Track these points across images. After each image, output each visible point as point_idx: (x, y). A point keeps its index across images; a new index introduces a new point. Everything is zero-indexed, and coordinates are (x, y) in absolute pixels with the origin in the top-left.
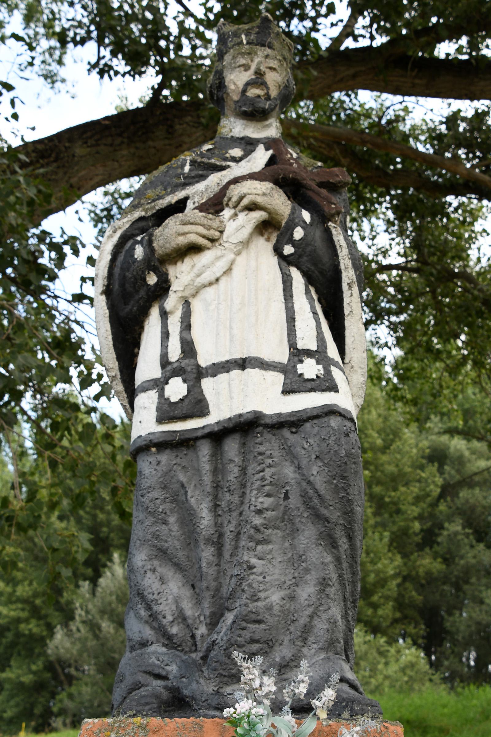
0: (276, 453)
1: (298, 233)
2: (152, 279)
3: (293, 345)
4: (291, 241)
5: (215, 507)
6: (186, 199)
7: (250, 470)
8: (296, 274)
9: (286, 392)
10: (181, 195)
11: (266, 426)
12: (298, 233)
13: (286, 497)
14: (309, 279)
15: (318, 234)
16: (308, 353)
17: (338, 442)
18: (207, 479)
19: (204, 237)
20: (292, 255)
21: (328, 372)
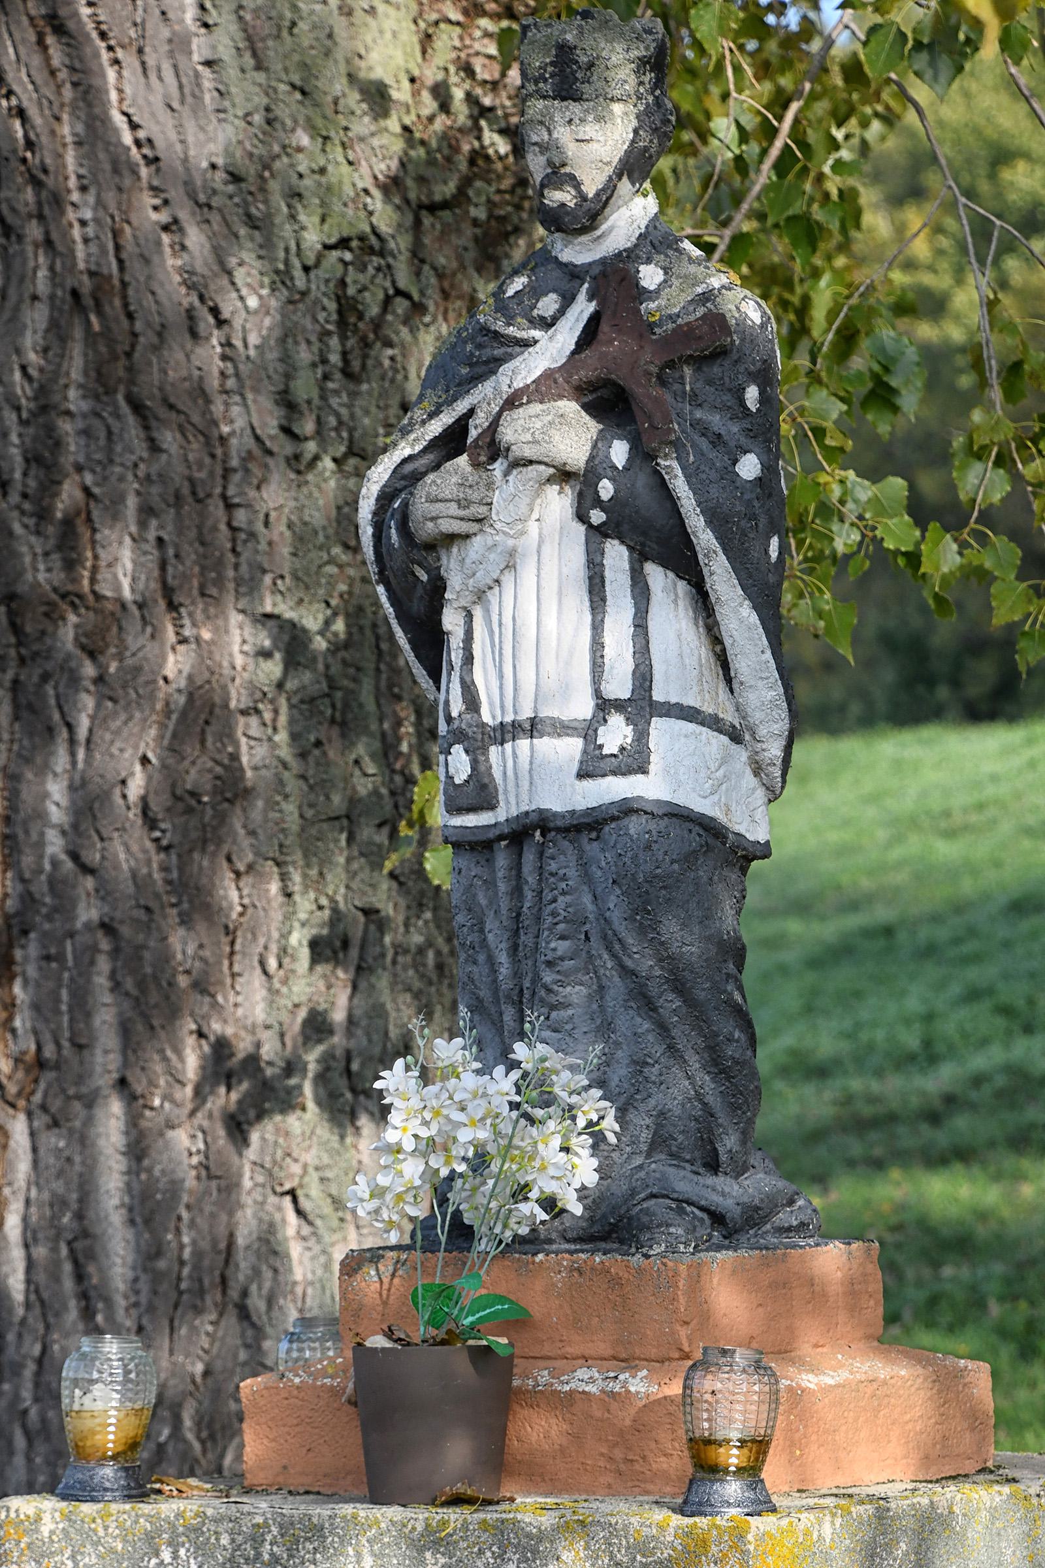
0: (572, 873)
1: (606, 489)
2: (424, 577)
3: (598, 694)
4: (598, 503)
5: (514, 949)
6: (471, 412)
7: (548, 896)
8: (616, 556)
9: (583, 774)
10: (462, 407)
11: (558, 830)
12: (606, 489)
13: (587, 938)
14: (640, 556)
15: (642, 480)
16: (619, 705)
17: (635, 857)
18: (504, 904)
19: (462, 519)
20: (604, 524)
21: (642, 736)
